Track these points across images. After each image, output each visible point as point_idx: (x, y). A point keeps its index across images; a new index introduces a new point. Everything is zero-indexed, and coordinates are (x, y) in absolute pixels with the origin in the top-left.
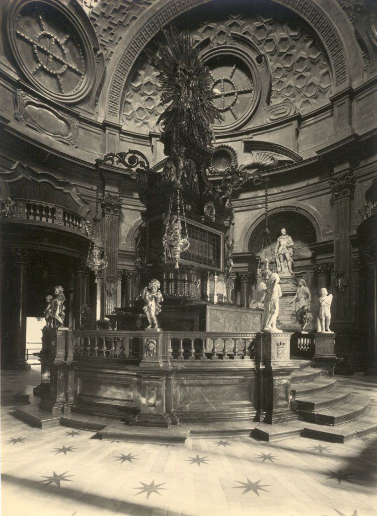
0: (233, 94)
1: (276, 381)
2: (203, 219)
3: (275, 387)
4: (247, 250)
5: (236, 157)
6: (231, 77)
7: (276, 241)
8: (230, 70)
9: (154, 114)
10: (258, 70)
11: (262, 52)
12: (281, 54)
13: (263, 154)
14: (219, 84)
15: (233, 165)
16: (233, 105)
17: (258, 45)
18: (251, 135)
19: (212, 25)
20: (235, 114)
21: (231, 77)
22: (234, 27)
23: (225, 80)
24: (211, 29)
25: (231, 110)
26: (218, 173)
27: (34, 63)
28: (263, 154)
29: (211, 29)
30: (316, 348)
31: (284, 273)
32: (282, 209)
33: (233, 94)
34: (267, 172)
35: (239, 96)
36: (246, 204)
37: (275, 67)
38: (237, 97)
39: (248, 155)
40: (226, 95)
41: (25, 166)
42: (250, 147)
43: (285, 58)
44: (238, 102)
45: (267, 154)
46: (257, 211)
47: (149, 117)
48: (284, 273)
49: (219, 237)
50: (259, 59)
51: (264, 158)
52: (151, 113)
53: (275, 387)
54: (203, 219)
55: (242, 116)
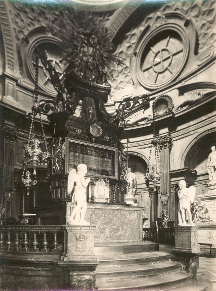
0: (169, 58)
1: (75, 276)
2: (94, 139)
3: (73, 283)
4: (183, 167)
5: (172, 101)
6: (167, 46)
7: (208, 157)
8: (165, 41)
9: (117, 89)
10: (187, 33)
11: (188, 18)
12: (204, 13)
13: (192, 93)
14: (159, 55)
15: (170, 108)
16: (169, 66)
17: (186, 14)
18: (183, 82)
19: (151, 15)
20: (171, 71)
21: (167, 46)
22: (167, 9)
23: (163, 50)
24: (150, 18)
25: (168, 70)
26: (159, 115)
27: (45, 78)
28: (192, 93)
29: (150, 18)
30: (176, 241)
31: (214, 181)
32: (210, 131)
33: (169, 58)
34: (196, 105)
35: (174, 57)
36: (181, 133)
37: (201, 25)
38: (172, 59)
39: (182, 97)
40: (164, 61)
41: (39, 136)
42: (182, 91)
43: (208, 15)
44: (173, 62)
45: (195, 92)
46: (190, 137)
47: (114, 92)
48: (214, 181)
49: (113, 152)
50: (188, 23)
51: (193, 96)
52: (116, 89)
53: (73, 283)
54: (94, 139)
55: (176, 71)
